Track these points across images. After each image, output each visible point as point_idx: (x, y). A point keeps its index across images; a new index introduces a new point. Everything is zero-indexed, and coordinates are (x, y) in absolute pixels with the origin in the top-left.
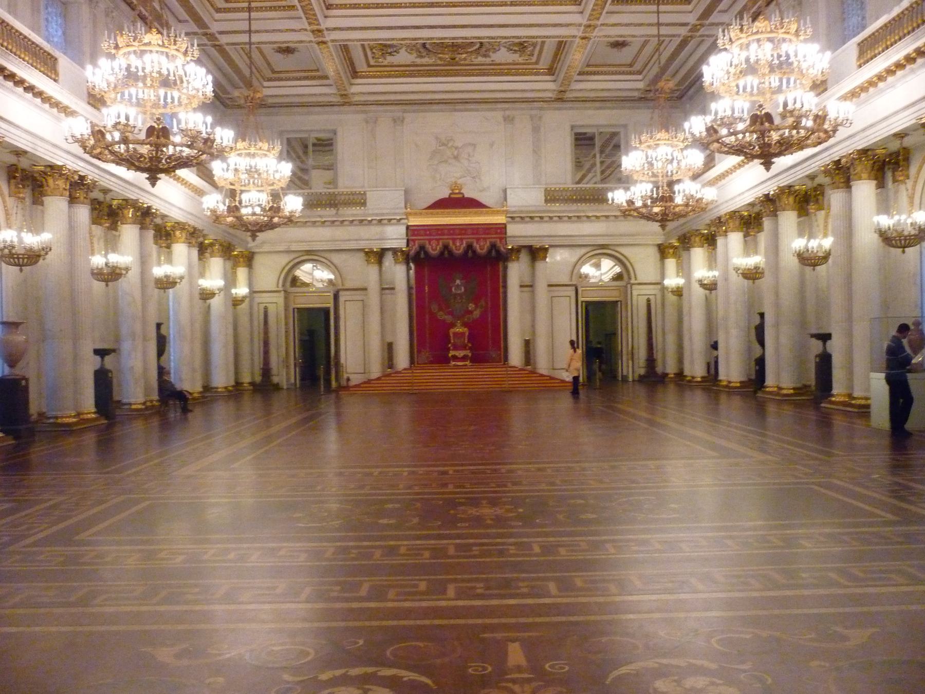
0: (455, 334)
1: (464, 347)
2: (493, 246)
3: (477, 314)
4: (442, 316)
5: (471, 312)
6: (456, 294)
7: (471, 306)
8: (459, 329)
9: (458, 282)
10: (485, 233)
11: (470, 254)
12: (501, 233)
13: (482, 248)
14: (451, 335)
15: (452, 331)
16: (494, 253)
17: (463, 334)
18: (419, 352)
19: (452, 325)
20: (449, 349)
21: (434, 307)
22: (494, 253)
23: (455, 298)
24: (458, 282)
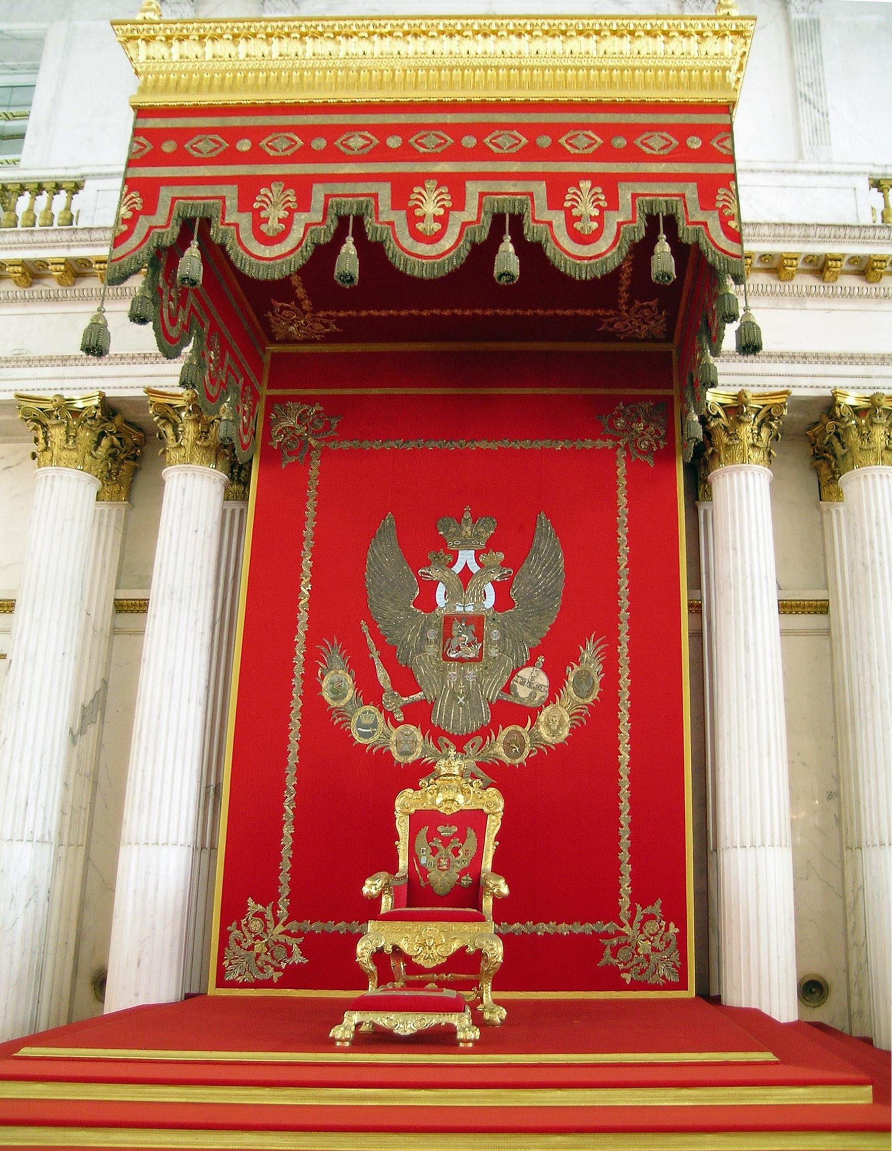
0: (422, 820)
1: (464, 900)
2: (659, 223)
3: (555, 726)
4: (367, 727)
5: (524, 714)
6: (448, 621)
7: (532, 683)
8: (455, 788)
9: (466, 558)
10: (605, 154)
11: (508, 261)
12: (707, 154)
13: (586, 237)
14: (402, 827)
15: (406, 803)
16: (663, 257)
17: (474, 820)
18: (232, 911)
19: (417, 774)
20: (369, 910)
21: (337, 682)
22: (663, 257)
23: (447, 634)
24: (466, 558)
